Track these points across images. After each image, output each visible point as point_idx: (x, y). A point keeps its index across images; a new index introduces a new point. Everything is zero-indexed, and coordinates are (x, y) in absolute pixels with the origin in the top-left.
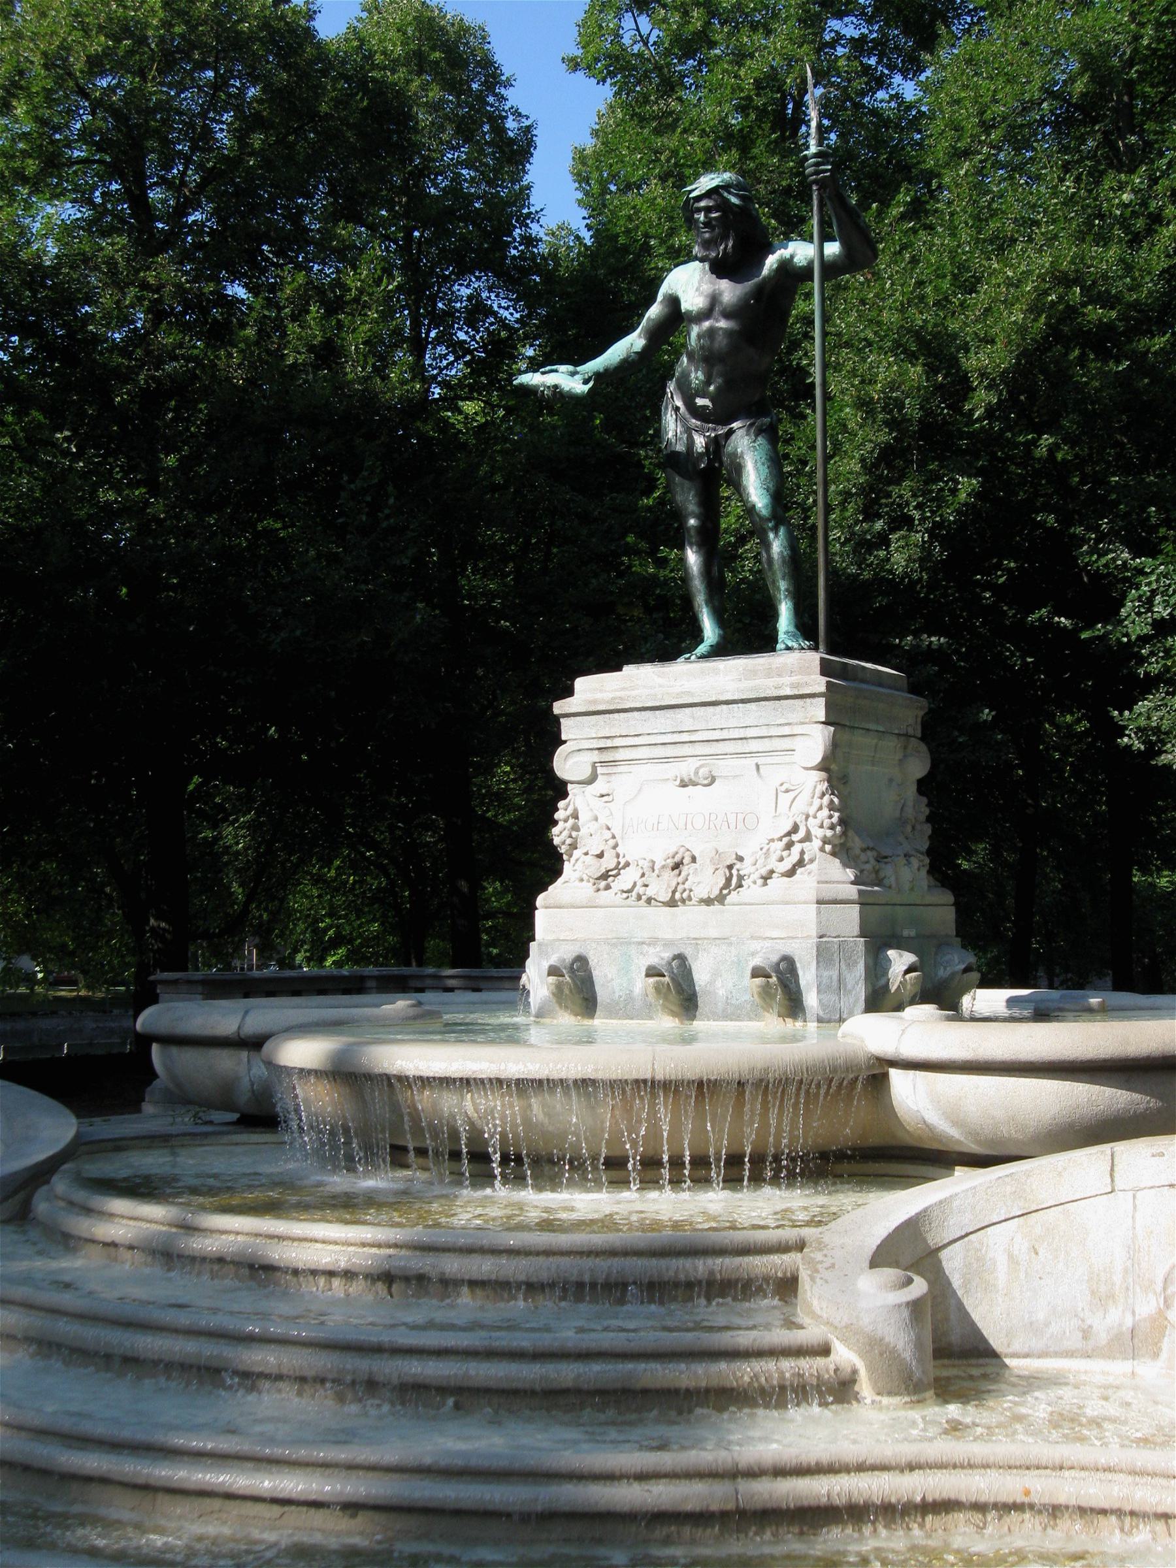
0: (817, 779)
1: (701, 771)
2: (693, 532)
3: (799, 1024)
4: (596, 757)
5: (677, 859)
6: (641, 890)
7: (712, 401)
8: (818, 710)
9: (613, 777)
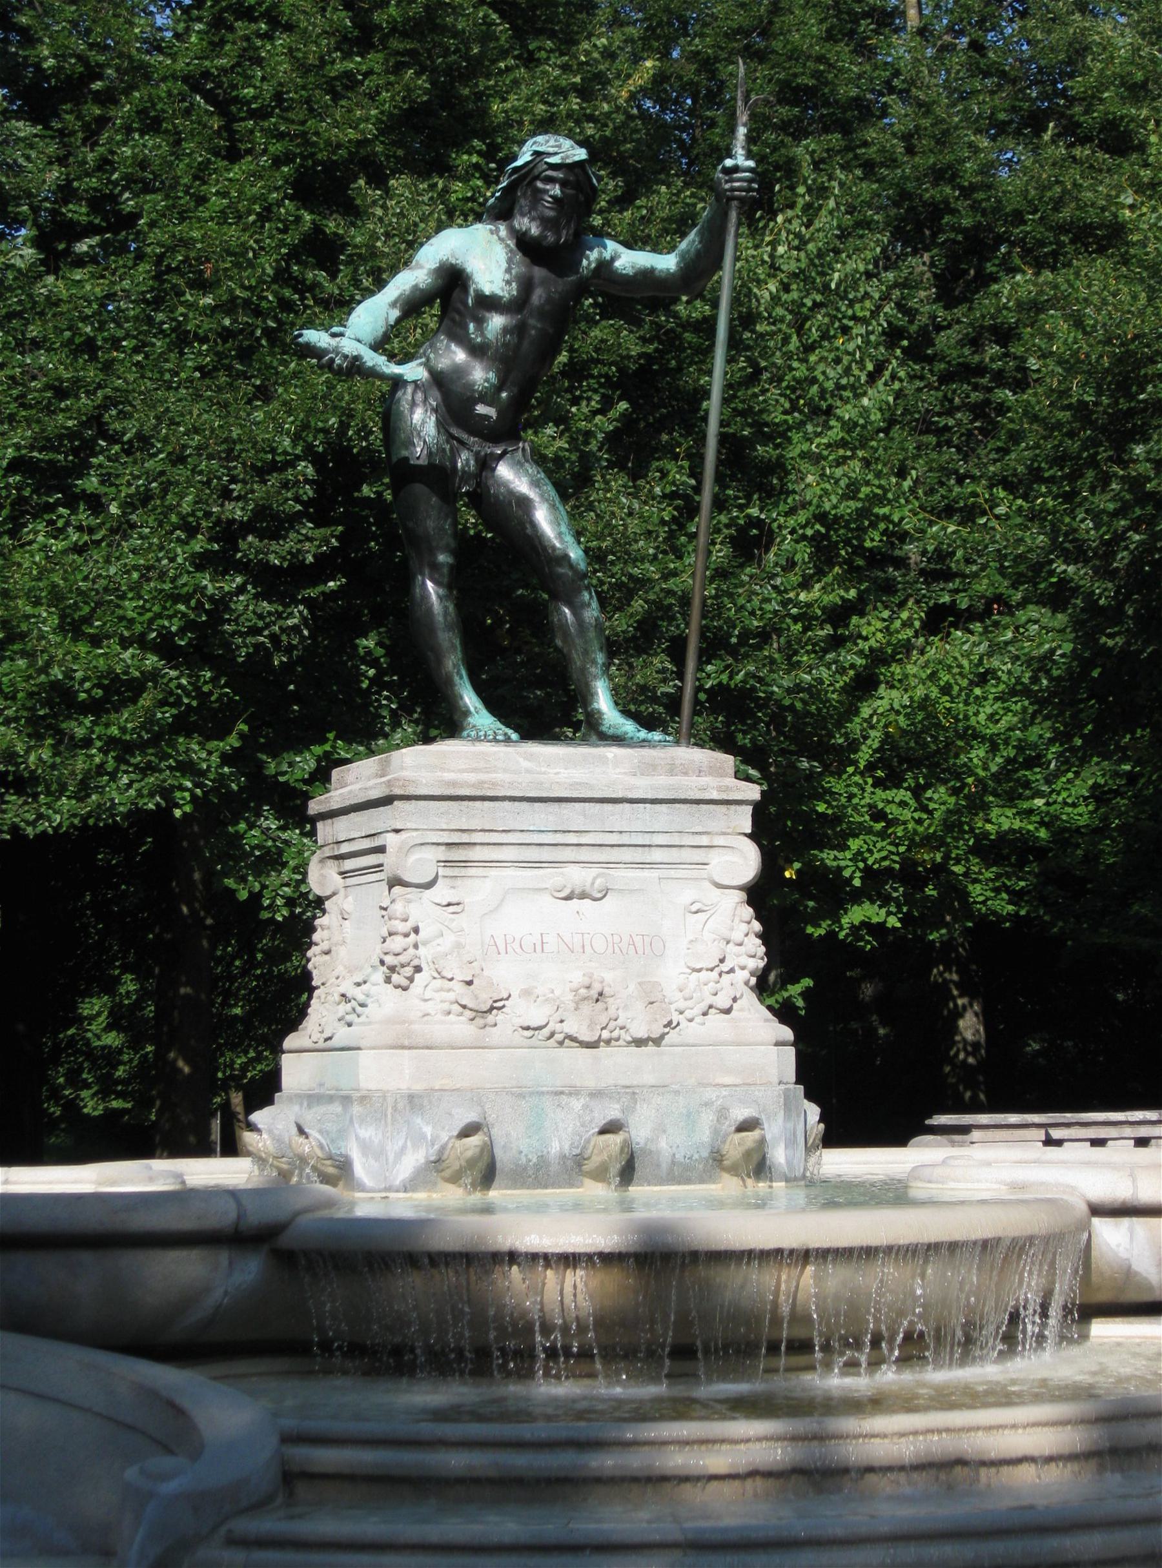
0: (737, 900)
1: (598, 881)
2: (445, 570)
3: (762, 1185)
4: (442, 853)
5: (597, 987)
6: (558, 1027)
7: (499, 412)
8: (744, 820)
9: (459, 882)
